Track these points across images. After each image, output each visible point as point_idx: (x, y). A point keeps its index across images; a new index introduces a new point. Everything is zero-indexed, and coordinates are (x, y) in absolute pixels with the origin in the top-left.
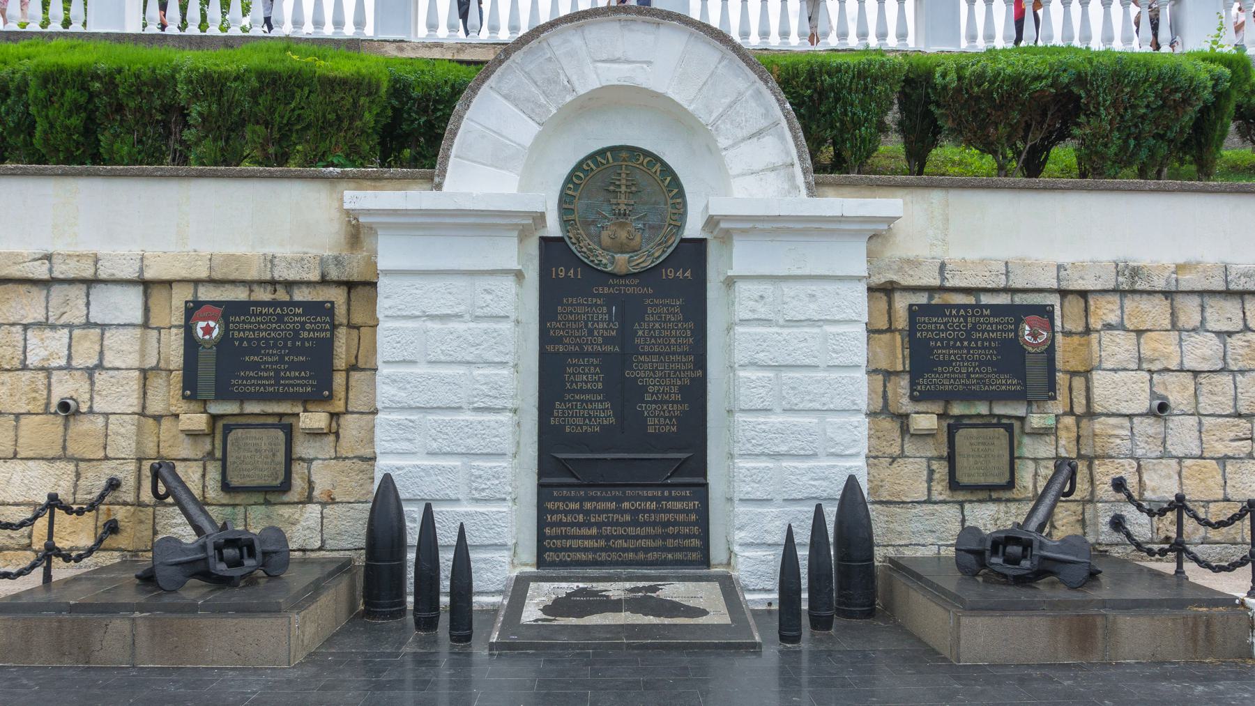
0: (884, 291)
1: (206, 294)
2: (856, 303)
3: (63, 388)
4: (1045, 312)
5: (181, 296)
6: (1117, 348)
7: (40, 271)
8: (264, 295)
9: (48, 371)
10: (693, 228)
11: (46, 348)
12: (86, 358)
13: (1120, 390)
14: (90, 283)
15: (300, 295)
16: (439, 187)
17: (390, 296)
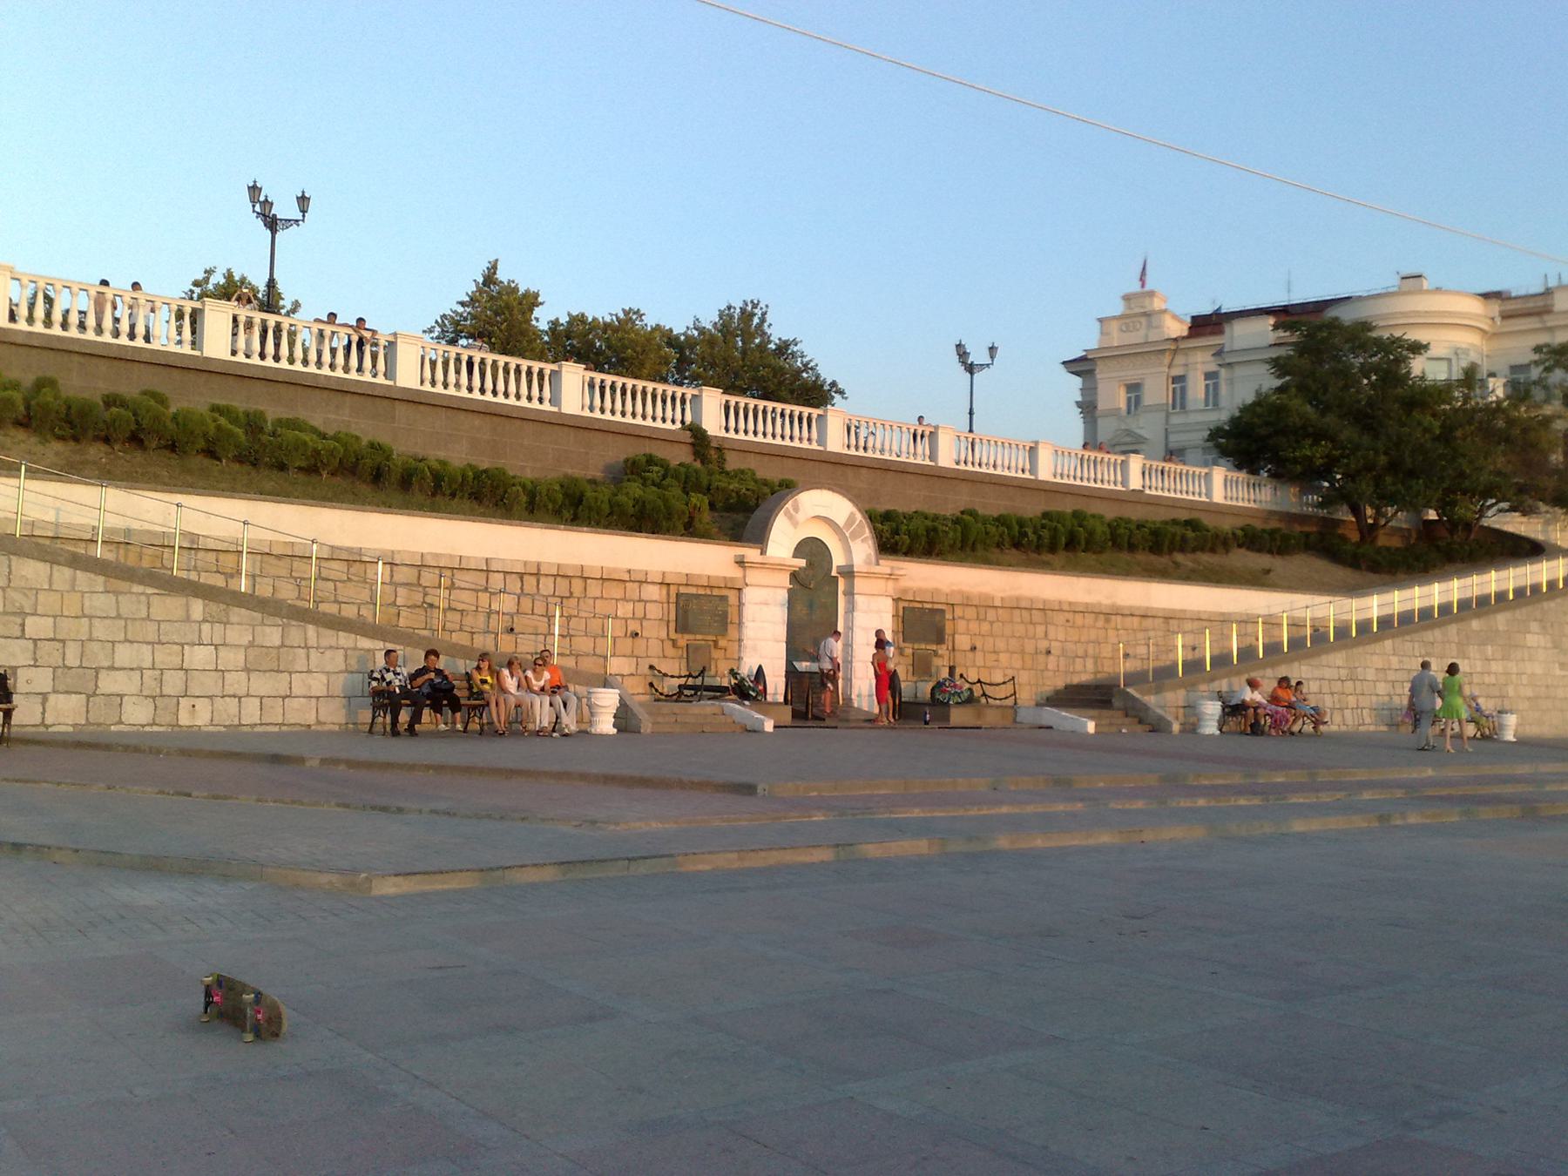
0: (896, 600)
1: (683, 590)
2: (889, 603)
3: (634, 626)
4: (943, 611)
5: (673, 589)
6: (961, 625)
7: (626, 577)
8: (701, 592)
9: (626, 620)
10: (834, 573)
11: (625, 610)
12: (639, 614)
13: (963, 642)
14: (641, 582)
15: (716, 592)
16: (763, 553)
17: (750, 595)
